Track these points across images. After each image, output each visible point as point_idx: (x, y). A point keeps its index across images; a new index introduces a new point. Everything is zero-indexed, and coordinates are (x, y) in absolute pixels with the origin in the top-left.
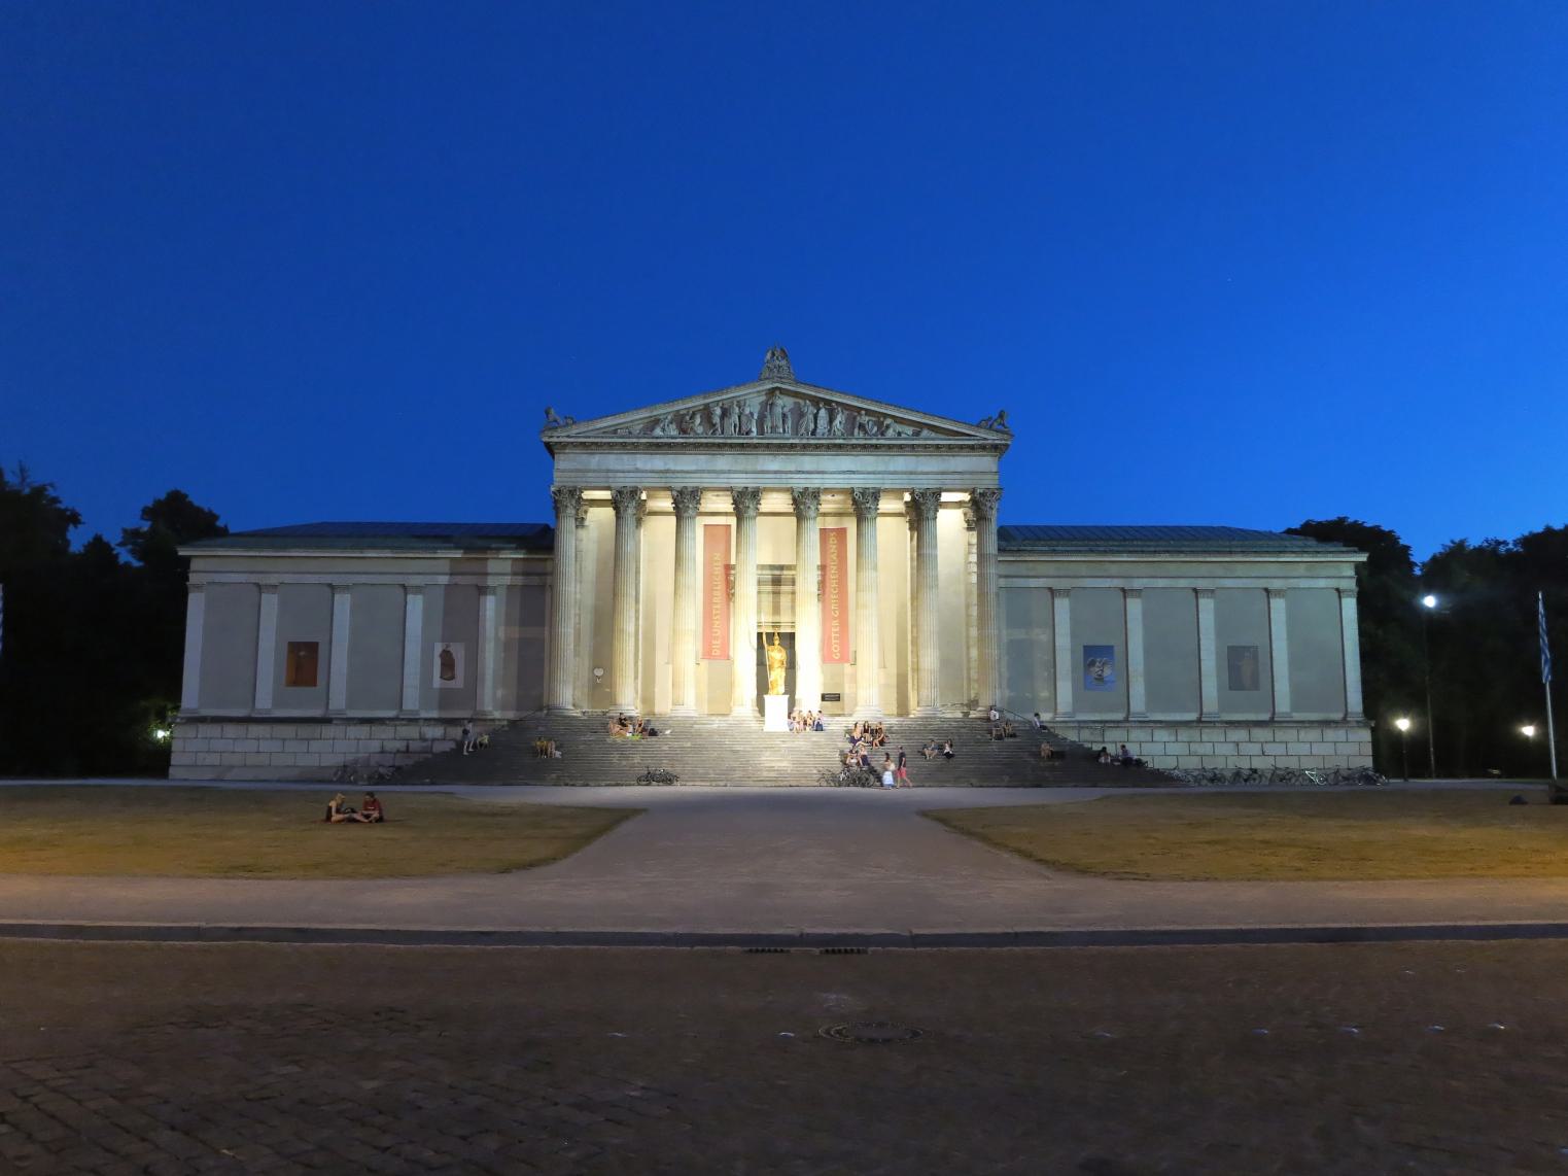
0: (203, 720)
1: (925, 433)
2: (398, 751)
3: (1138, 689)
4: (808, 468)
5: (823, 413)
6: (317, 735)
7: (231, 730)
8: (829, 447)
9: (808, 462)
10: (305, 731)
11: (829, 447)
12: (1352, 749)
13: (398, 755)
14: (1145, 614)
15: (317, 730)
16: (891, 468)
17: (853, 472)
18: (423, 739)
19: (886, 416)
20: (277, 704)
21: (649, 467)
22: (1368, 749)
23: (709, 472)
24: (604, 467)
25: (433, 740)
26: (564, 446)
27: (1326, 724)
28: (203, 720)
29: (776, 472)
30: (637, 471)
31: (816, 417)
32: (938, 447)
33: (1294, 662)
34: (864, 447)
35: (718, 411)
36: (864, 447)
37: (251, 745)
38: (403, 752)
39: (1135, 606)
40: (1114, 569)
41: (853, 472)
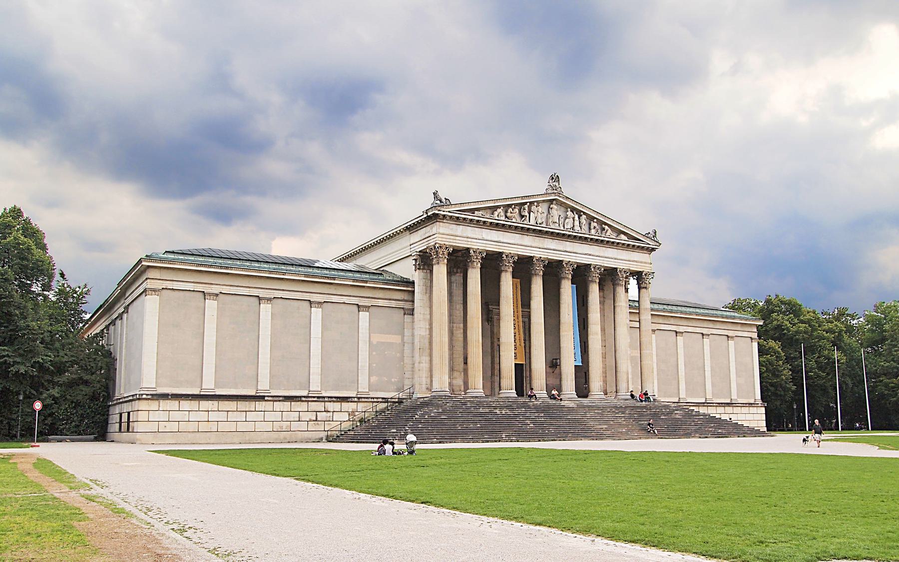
0: (165, 396)
1: (623, 237)
5: (577, 216)
7: (186, 405)
10: (243, 405)
12: (757, 417)
15: (251, 405)
16: (606, 255)
19: (606, 224)
20: (217, 385)
22: (764, 417)
24: (465, 235)
27: (750, 405)
28: (165, 396)
31: (573, 218)
33: (738, 375)
37: (203, 416)
40: (672, 321)
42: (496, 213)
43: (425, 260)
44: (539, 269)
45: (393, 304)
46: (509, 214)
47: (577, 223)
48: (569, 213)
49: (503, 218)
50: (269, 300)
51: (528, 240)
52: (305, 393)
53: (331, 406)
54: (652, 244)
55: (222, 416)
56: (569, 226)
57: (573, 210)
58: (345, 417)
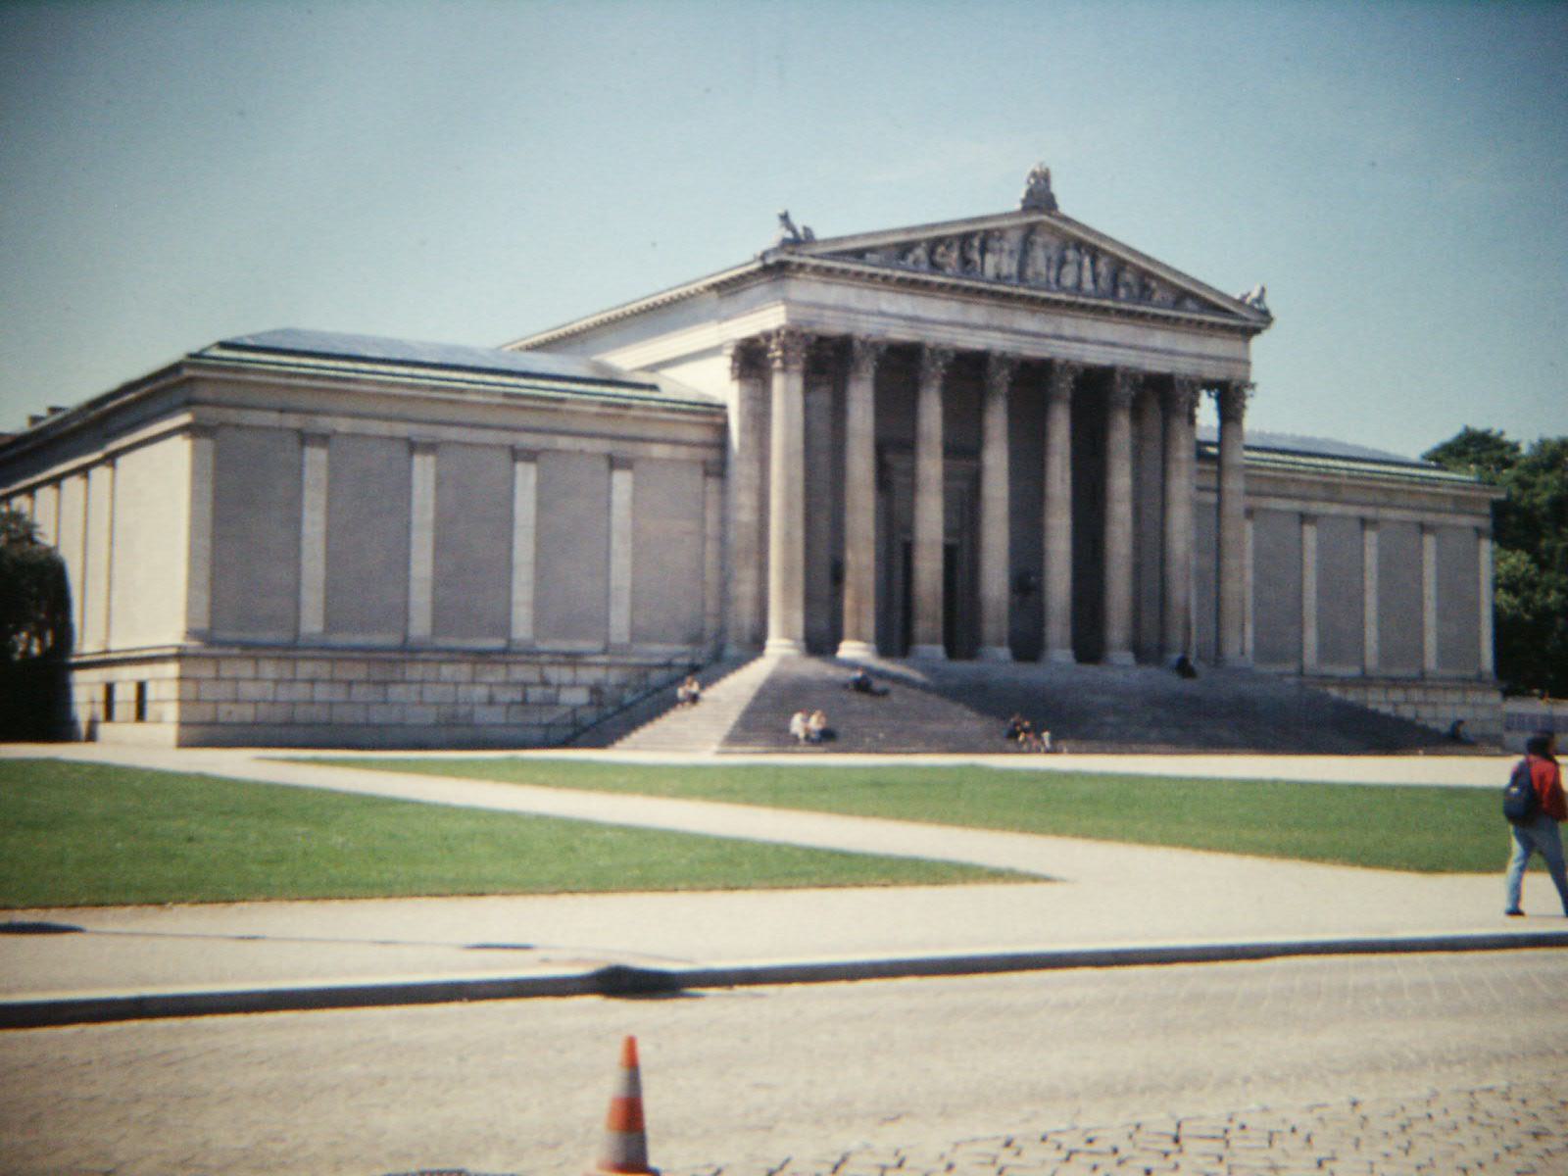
1: (1189, 304)
2: (512, 703)
3: (1311, 638)
4: (1068, 331)
5: (1087, 261)
6: (398, 677)
8: (1095, 309)
9: (1069, 325)
11: (1095, 309)
13: (514, 709)
14: (1321, 547)
17: (1113, 345)
18: (545, 683)
21: (893, 309)
23: (965, 325)
25: (559, 686)
26: (801, 266)
29: (1036, 335)
30: (882, 314)
31: (1080, 266)
32: (1200, 323)
34: (1130, 314)
35: (976, 243)
36: (1130, 314)
37: (301, 691)
38: (518, 703)
39: (1310, 534)
41: (1113, 345)
42: (911, 258)
43: (751, 359)
44: (1001, 378)
45: (682, 452)
46: (938, 258)
47: (1087, 275)
48: (1071, 254)
49: (925, 266)
50: (431, 447)
51: (977, 313)
52: (498, 643)
53: (555, 674)
54: (1254, 319)
55: (339, 693)
56: (1069, 280)
57: (1079, 245)
58: (580, 696)
